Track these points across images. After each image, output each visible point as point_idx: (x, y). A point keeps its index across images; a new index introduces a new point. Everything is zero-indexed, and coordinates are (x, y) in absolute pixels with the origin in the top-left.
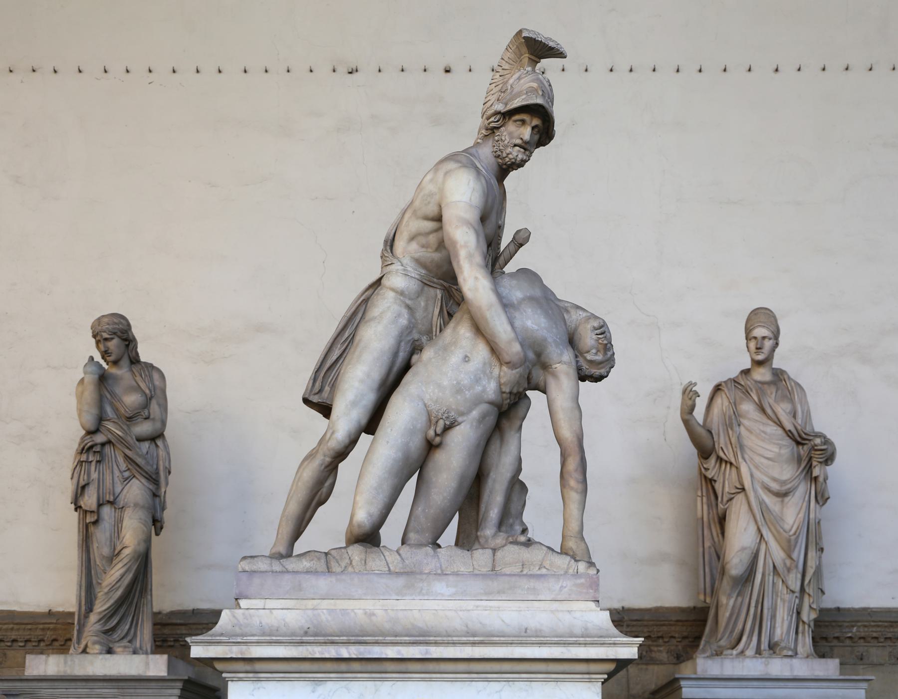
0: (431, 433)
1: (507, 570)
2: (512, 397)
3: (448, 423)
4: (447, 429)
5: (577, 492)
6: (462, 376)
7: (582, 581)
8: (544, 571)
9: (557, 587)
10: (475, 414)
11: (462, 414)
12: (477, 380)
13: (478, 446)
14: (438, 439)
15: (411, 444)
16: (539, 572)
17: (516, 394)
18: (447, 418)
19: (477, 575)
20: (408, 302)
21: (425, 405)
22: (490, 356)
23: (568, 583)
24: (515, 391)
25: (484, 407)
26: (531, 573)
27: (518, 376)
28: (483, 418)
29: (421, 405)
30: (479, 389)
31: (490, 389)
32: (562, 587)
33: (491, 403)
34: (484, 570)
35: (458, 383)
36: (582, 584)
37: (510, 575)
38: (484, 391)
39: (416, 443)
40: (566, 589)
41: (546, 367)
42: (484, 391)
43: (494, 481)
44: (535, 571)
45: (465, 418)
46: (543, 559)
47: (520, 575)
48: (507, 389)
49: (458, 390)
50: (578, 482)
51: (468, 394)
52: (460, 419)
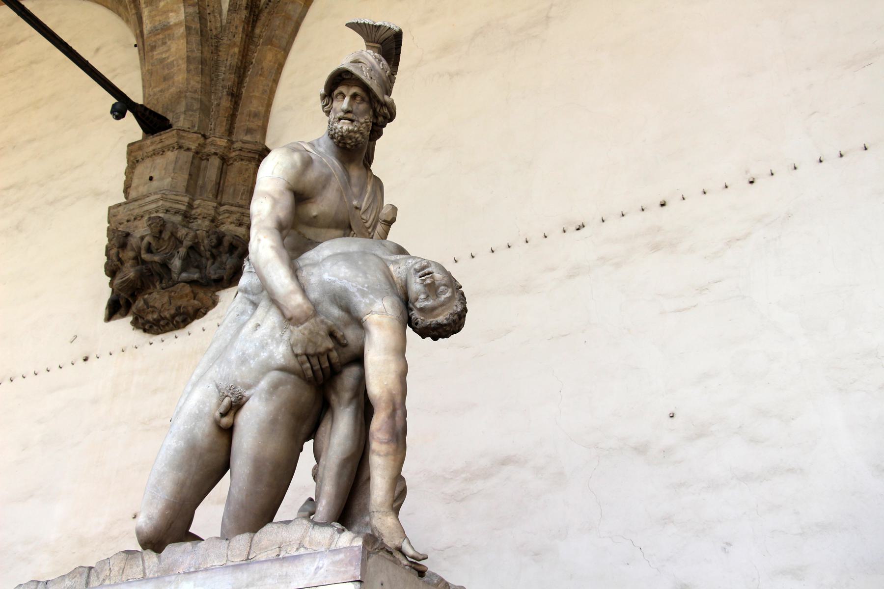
0: (217, 414)
1: (262, 557)
2: (315, 361)
3: (233, 399)
4: (236, 406)
5: (379, 455)
6: (247, 345)
7: (342, 556)
8: (302, 551)
9: (313, 569)
10: (264, 384)
11: (249, 387)
12: (263, 346)
13: (274, 421)
14: (225, 421)
15: (197, 430)
16: (296, 554)
17: (318, 355)
18: (232, 394)
19: (227, 567)
20: (251, 297)
21: (217, 387)
22: (281, 318)
23: (325, 562)
24: (311, 351)
25: (275, 375)
26: (287, 555)
27: (306, 332)
28: (275, 387)
29: (212, 387)
30: (264, 355)
31: (280, 353)
32: (318, 568)
33: (282, 369)
34: (237, 560)
35: (243, 354)
36: (342, 561)
37: (266, 561)
38: (271, 356)
39: (204, 429)
40: (322, 570)
41: (359, 323)
42: (271, 356)
43: (324, 468)
44: (294, 553)
45: (252, 391)
46: (303, 537)
47: (278, 558)
48: (299, 351)
49: (243, 360)
50: (381, 443)
51: (253, 363)
52: (247, 394)
